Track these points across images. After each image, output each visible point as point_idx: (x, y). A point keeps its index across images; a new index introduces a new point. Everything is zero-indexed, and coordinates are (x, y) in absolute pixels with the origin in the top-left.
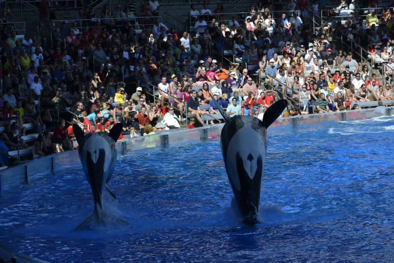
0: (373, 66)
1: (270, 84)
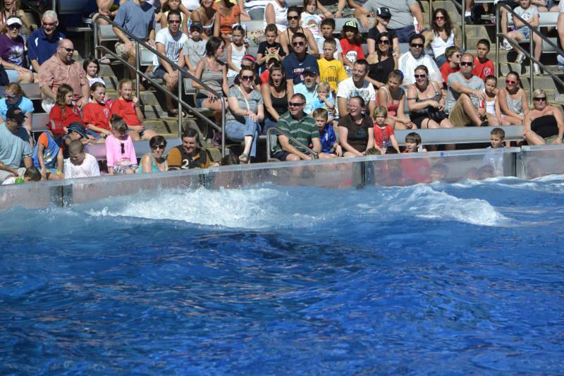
0: (468, 14)
1: (129, 63)
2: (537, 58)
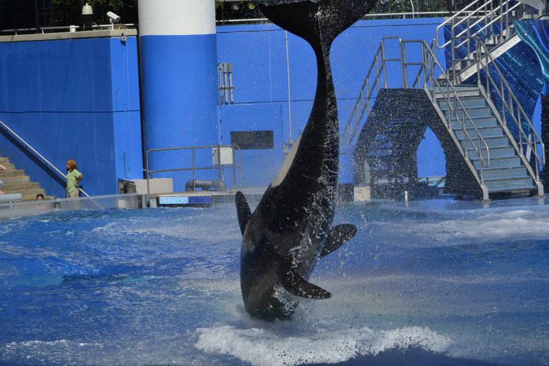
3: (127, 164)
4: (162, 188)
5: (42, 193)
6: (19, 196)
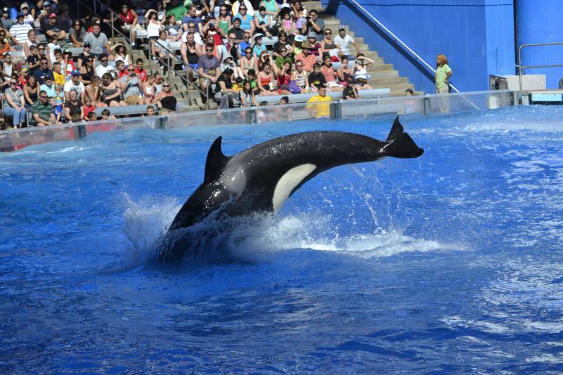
0: (133, 44)
2: (173, 67)
3: (499, 61)
4: (534, 83)
5: (410, 88)
6: (387, 91)
